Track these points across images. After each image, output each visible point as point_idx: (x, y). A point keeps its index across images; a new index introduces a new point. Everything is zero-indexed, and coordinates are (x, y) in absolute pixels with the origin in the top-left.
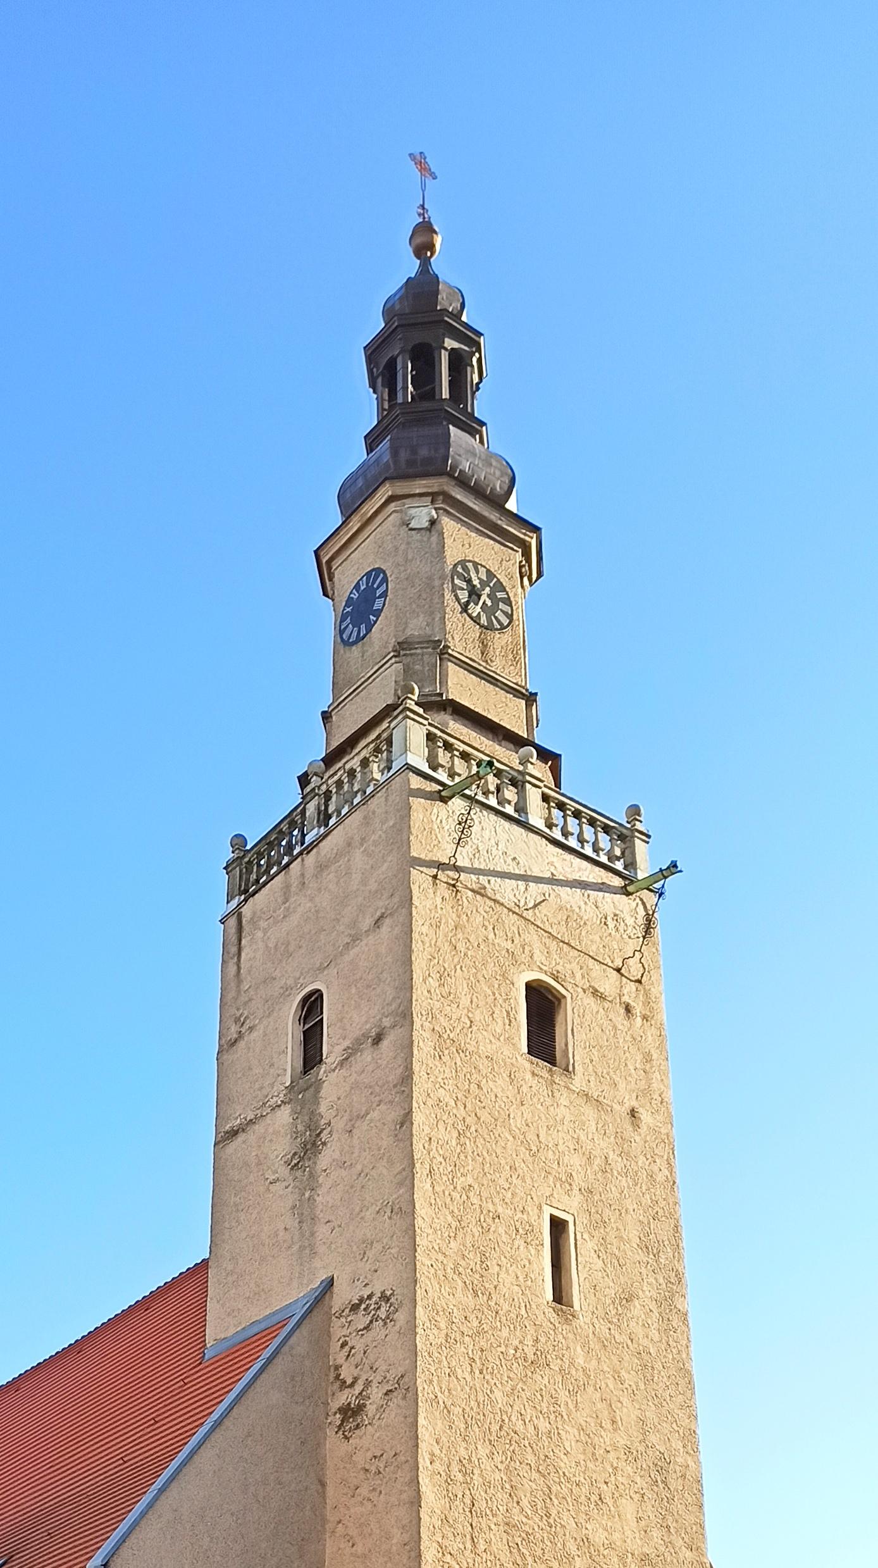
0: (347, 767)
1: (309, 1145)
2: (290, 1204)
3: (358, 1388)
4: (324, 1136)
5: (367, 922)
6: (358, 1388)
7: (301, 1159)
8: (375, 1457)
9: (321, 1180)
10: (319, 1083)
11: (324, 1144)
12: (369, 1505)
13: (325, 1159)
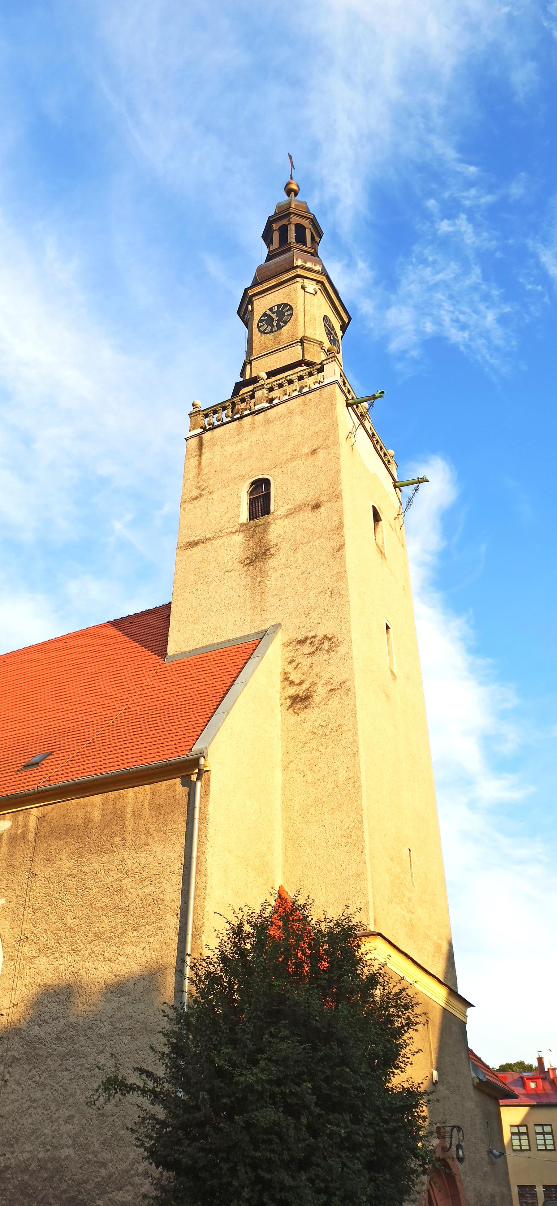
0: (288, 378)
1: (259, 555)
2: (244, 583)
3: (305, 686)
4: (272, 551)
5: (306, 450)
6: (305, 686)
7: (252, 561)
8: (322, 726)
9: (270, 573)
10: (266, 526)
11: (272, 555)
12: (318, 753)
13: (272, 562)
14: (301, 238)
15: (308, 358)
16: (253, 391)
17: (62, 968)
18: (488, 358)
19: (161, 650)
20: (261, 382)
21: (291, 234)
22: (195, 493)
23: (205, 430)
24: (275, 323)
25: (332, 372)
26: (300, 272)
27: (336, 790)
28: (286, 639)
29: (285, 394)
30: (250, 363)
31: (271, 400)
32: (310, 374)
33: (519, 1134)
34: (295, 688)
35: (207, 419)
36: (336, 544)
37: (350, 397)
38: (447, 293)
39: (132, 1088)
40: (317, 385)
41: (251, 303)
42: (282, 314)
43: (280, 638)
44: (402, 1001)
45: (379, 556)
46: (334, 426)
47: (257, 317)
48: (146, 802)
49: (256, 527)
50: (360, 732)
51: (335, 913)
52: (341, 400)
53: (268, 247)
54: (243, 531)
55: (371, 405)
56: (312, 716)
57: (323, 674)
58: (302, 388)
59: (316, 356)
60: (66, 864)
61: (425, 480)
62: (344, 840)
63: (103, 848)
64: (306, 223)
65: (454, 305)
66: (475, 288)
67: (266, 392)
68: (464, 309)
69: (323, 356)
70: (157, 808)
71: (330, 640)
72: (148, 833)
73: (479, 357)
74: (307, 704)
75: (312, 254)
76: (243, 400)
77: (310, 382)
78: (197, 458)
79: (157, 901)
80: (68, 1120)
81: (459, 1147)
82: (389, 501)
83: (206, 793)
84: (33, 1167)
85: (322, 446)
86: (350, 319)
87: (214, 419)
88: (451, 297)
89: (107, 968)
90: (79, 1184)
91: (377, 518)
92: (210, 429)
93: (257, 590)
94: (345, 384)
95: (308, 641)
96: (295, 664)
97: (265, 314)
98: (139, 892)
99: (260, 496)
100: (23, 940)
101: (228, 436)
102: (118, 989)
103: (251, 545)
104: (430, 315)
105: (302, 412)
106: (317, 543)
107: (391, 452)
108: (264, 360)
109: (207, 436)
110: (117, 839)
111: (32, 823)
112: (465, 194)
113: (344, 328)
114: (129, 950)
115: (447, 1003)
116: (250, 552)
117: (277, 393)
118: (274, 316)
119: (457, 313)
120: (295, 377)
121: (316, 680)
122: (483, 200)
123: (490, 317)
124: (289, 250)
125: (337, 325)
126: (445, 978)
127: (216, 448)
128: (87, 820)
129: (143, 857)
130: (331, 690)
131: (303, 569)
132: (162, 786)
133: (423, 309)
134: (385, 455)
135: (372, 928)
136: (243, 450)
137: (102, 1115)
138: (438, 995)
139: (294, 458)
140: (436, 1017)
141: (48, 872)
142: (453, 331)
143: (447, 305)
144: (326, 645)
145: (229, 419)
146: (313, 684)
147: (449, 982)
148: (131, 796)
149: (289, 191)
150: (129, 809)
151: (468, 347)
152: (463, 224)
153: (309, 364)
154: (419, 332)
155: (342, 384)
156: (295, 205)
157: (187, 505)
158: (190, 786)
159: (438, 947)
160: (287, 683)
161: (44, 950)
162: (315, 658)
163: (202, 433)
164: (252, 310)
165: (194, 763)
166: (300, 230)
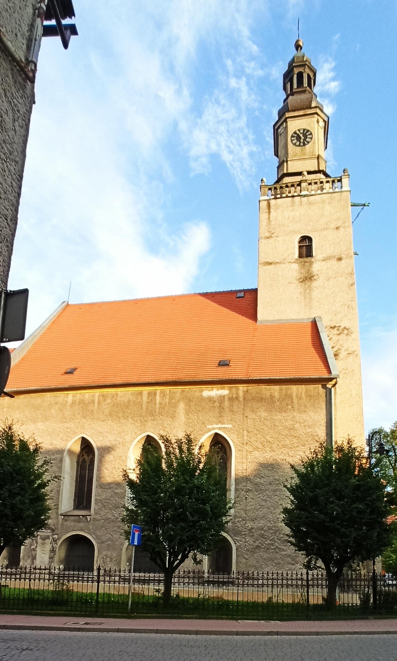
1: (308, 278)
4: (315, 277)
5: (333, 226)
9: (314, 289)
10: (311, 263)
11: (315, 280)
13: (315, 284)
22: (267, 234)
24: (302, 141)
49: (305, 262)
54: (298, 263)
60: (264, 414)
63: (281, 410)
71: (347, 329)
72: (305, 406)
78: (267, 214)
95: (336, 328)
97: (295, 133)
98: (304, 431)
99: (306, 247)
103: (302, 271)
105: (330, 203)
106: (340, 279)
108: (295, 162)
110: (290, 407)
111: (241, 394)
116: (302, 275)
118: (301, 135)
121: (340, 347)
128: (272, 397)
129: (304, 416)
131: (333, 291)
132: (311, 387)
139: (326, 229)
141: (254, 416)
144: (346, 332)
146: (339, 349)
148: (294, 389)
149: (298, 47)
150: (294, 395)
157: (262, 240)
161: (257, 449)
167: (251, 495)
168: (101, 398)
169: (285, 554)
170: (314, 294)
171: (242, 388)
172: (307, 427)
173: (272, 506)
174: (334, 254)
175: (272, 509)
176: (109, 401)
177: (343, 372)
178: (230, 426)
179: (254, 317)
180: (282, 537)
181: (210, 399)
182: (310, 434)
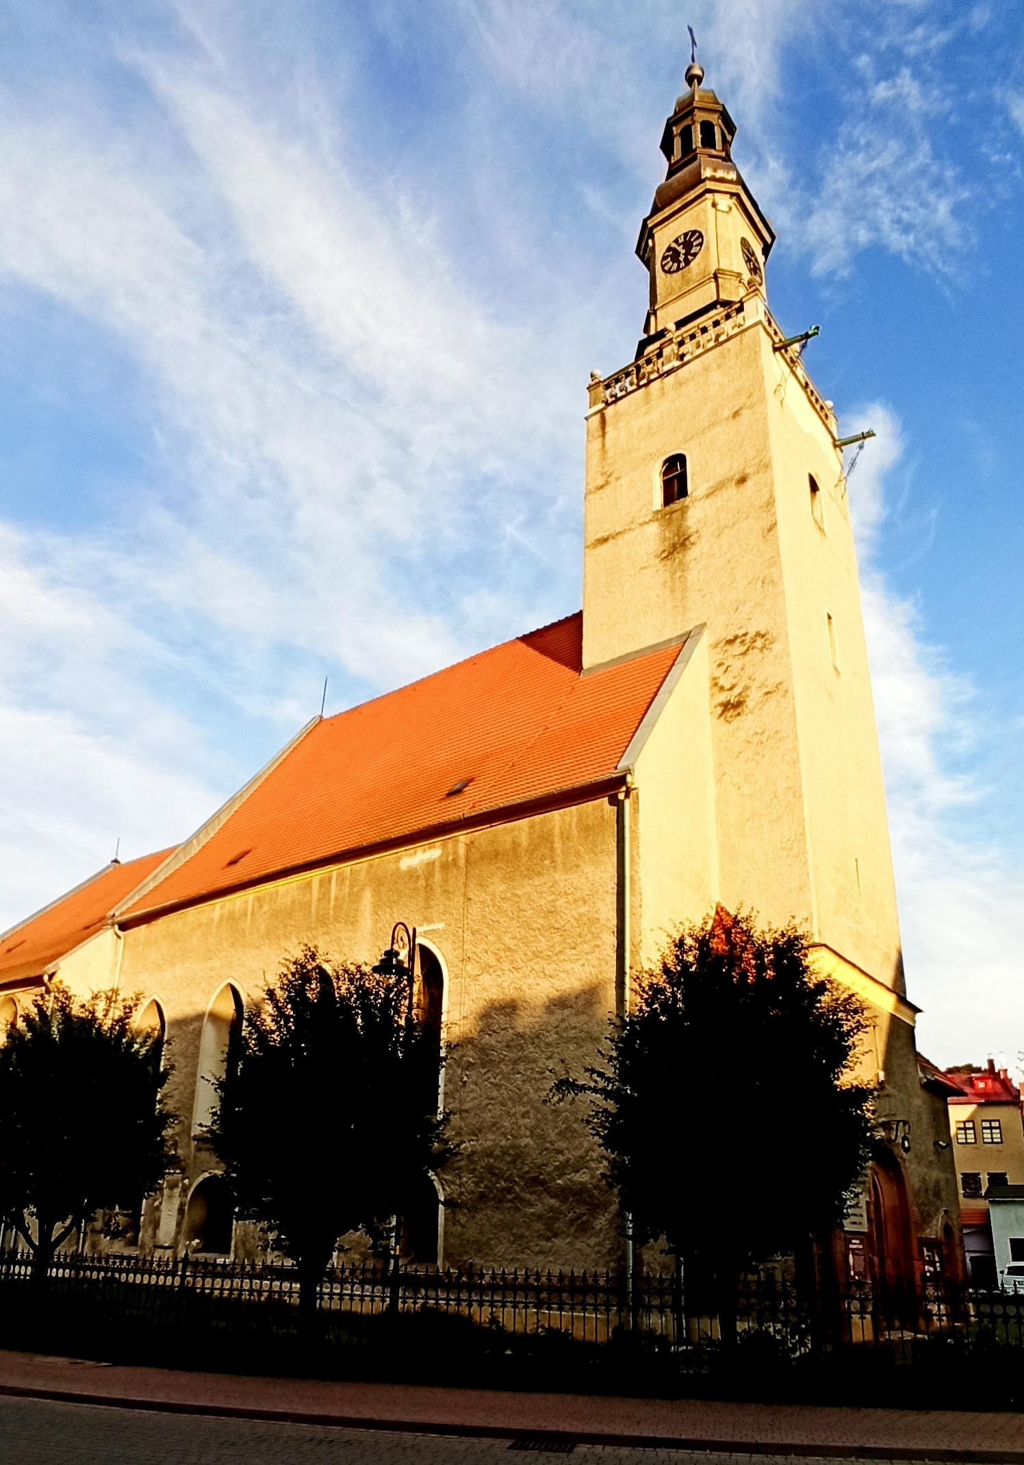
1: (678, 546)
2: (662, 580)
3: (737, 691)
4: (692, 539)
5: (727, 413)
6: (737, 691)
10: (684, 510)
11: (693, 544)
13: (692, 553)
14: (708, 141)
15: (723, 297)
16: (661, 348)
17: (505, 984)
18: (940, 265)
19: (575, 663)
20: (669, 336)
21: (696, 135)
22: (600, 481)
23: (607, 404)
24: (682, 258)
25: (756, 309)
26: (710, 185)
27: (775, 801)
28: (713, 640)
29: (698, 346)
30: (655, 313)
31: (682, 357)
32: (728, 317)
33: (965, 1129)
34: (725, 694)
35: (610, 389)
36: (766, 524)
37: (777, 340)
38: (885, 185)
39: (583, 1088)
40: (737, 330)
41: (652, 236)
42: (691, 243)
43: (706, 639)
44: (851, 1006)
45: (816, 533)
46: (759, 381)
47: (660, 252)
48: (574, 824)
49: (672, 513)
50: (800, 737)
51: (780, 925)
52: (766, 344)
53: (669, 159)
54: (657, 520)
55: (803, 347)
56: (747, 723)
57: (756, 676)
58: (718, 336)
59: (732, 292)
60: (500, 888)
61: (871, 434)
62: (785, 853)
63: (534, 871)
64: (714, 118)
65: (895, 200)
66: (922, 172)
67: (674, 346)
68: (908, 203)
69: (742, 292)
70: (586, 829)
71: (763, 636)
72: (578, 854)
73: (928, 267)
74: (739, 710)
75: (724, 159)
76: (649, 362)
77: (728, 327)
78: (600, 439)
79: (594, 921)
80: (525, 1115)
81: (904, 1138)
82: (828, 465)
83: (636, 810)
84: (497, 1152)
85: (746, 406)
86: (773, 237)
87: (616, 390)
88: (890, 189)
89: (548, 984)
90: (539, 1167)
91: (814, 487)
92: (613, 402)
93: (677, 587)
94: (770, 323)
96: (724, 667)
97: (669, 249)
98: (574, 912)
100: (466, 960)
101: (633, 408)
102: (559, 1004)
103: (667, 535)
104: (863, 218)
105: (719, 366)
106: (744, 524)
107: (829, 403)
109: (610, 411)
110: (547, 862)
111: (462, 850)
112: (910, 37)
113: (766, 251)
114: (568, 967)
115: (896, 1009)
116: (667, 543)
117: (689, 346)
118: (680, 249)
119: (898, 211)
120: (709, 324)
121: (749, 683)
122: (933, 42)
123: (943, 208)
124: (695, 158)
125: (757, 247)
126: (894, 985)
127: (621, 424)
128: (515, 845)
129: (574, 878)
130: (767, 693)
131: (729, 556)
133: (856, 212)
134: (822, 408)
135: (816, 940)
136: (651, 422)
137: (555, 1111)
138: (885, 1003)
139: (713, 424)
140: (884, 1023)
141: (483, 896)
142: (895, 236)
143: (886, 202)
144: (759, 643)
145: (634, 387)
146: (746, 688)
147: (899, 989)
148: (557, 817)
149: (691, 79)
150: (557, 832)
151: (913, 254)
152: (907, 83)
153: (726, 304)
154: (850, 243)
155: (766, 324)
156: (700, 97)
157: (592, 496)
158: (619, 805)
159: (887, 956)
160: (717, 689)
161: (486, 969)
162: (747, 658)
163: (604, 409)
164: (654, 247)
165: (621, 781)
166: (707, 128)
167: (474, 1074)
168: (256, 904)
169: (533, 1214)
170: (692, 576)
171: (462, 838)
172: (580, 903)
173: (510, 1098)
174: (731, 474)
175: (510, 1104)
176: (266, 907)
177: (756, 740)
178: (441, 926)
179: (576, 665)
180: (527, 1172)
181: (412, 874)
182: (585, 919)
